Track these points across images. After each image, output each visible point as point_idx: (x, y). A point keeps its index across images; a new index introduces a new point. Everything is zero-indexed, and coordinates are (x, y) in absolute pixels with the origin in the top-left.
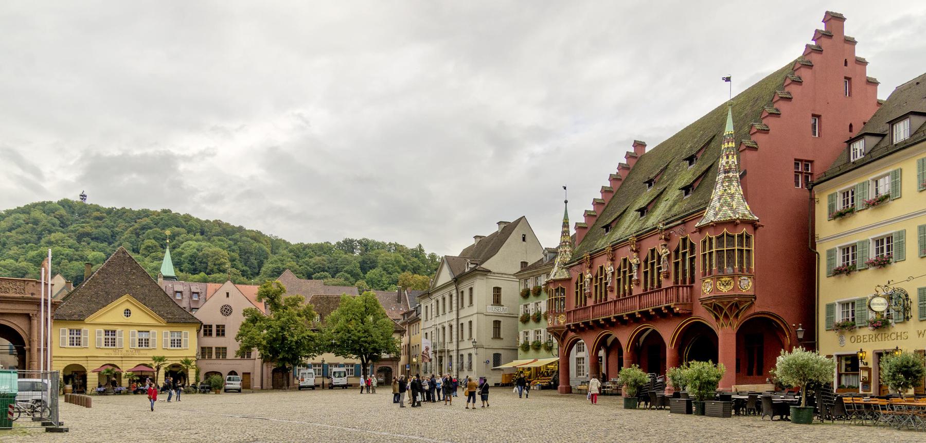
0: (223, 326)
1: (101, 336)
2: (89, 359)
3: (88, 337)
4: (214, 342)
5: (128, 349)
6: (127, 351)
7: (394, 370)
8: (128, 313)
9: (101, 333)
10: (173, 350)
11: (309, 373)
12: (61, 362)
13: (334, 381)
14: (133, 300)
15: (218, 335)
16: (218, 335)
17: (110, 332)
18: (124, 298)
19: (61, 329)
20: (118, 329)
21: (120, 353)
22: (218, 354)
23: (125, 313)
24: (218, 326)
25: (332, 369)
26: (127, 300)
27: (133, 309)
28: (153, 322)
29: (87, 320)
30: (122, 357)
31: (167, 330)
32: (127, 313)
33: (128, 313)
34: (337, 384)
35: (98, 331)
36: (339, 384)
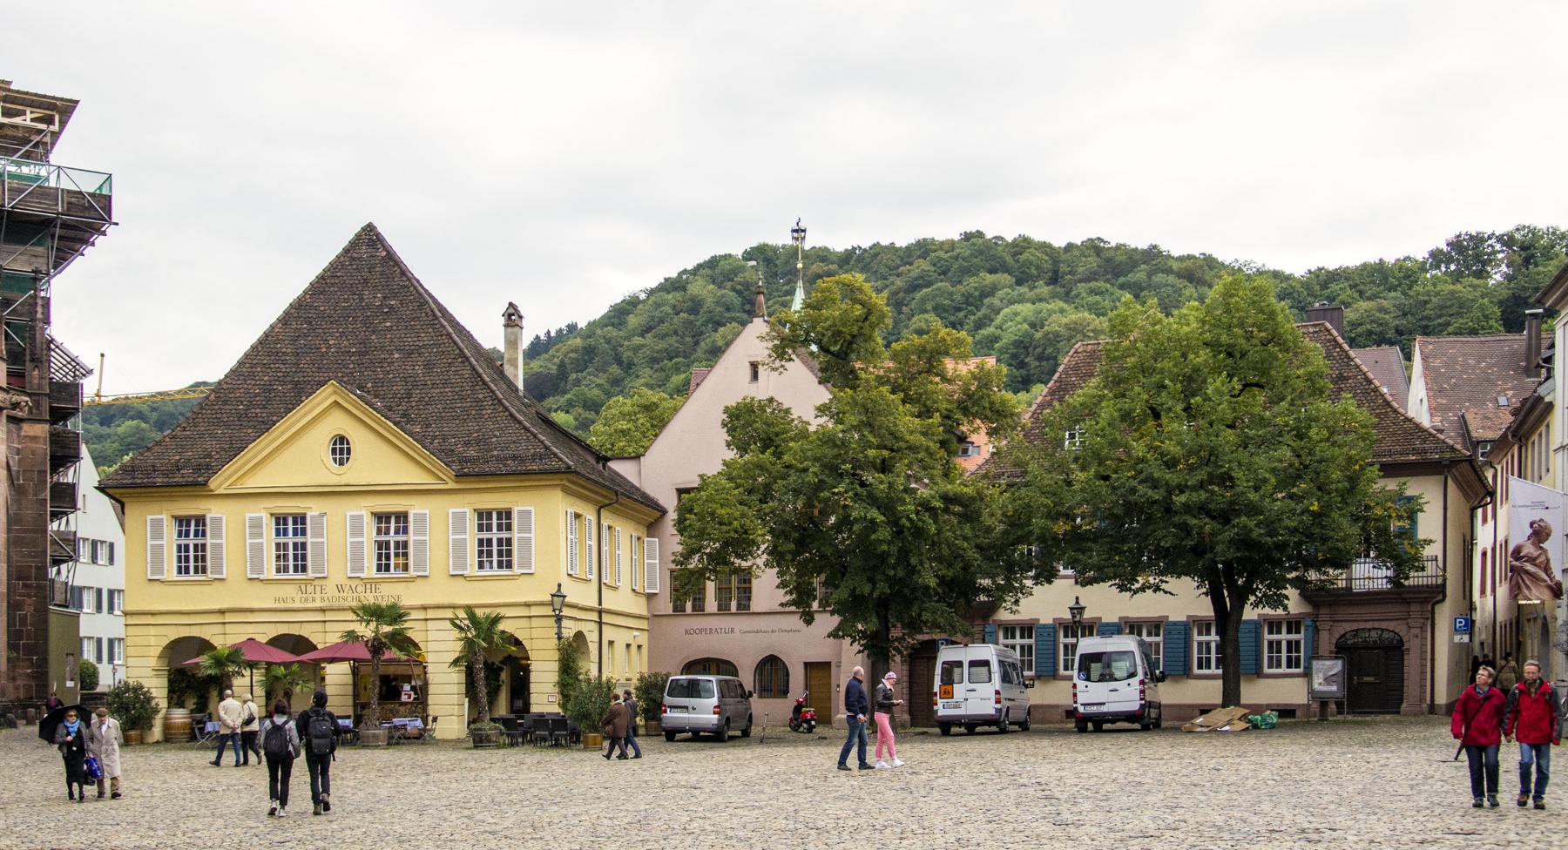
1: (261, 535)
2: (229, 618)
3: (223, 541)
5: (344, 581)
6: (340, 588)
7: (1412, 645)
8: (341, 449)
9: (261, 527)
10: (507, 578)
11: (973, 664)
12: (152, 630)
13: (1082, 698)
14: (350, 400)
17: (290, 521)
18: (325, 396)
19: (149, 517)
21: (318, 596)
23: (334, 451)
25: (1074, 646)
26: (336, 402)
27: (360, 440)
28: (416, 477)
29: (218, 483)
30: (323, 610)
31: (466, 506)
32: (342, 450)
33: (341, 449)
34: (1094, 709)
35: (251, 519)
36: (1104, 709)
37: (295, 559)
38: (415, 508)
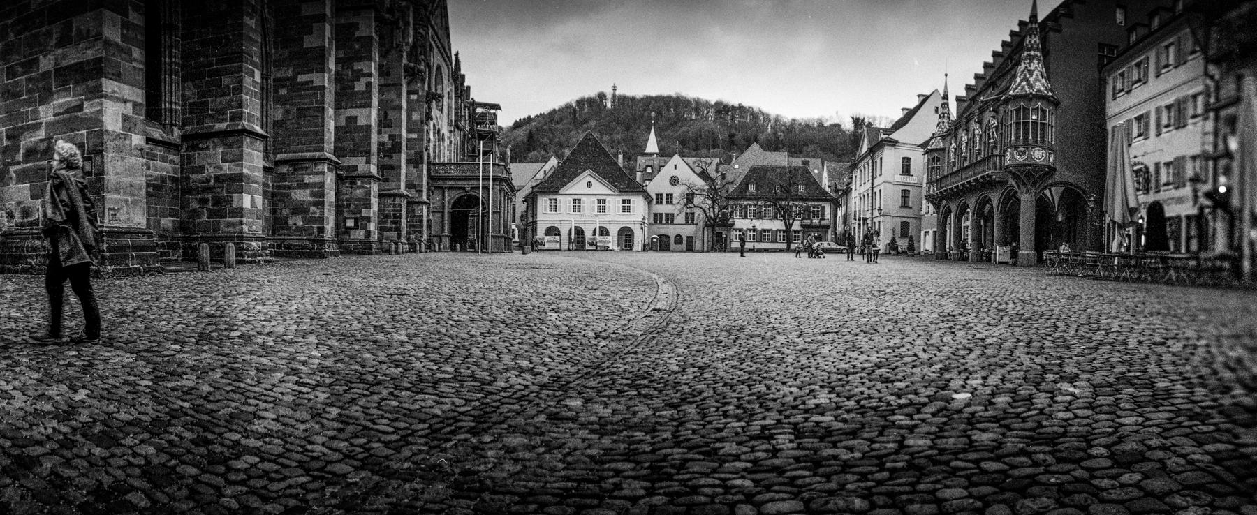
0: (672, 195)
4: (664, 209)
8: (590, 185)
15: (667, 203)
16: (667, 203)
18: (586, 173)
20: (583, 198)
22: (667, 219)
24: (667, 195)
27: (593, 181)
28: (610, 192)
29: (561, 191)
31: (620, 199)
33: (590, 185)
37: (577, 209)
38: (608, 198)
